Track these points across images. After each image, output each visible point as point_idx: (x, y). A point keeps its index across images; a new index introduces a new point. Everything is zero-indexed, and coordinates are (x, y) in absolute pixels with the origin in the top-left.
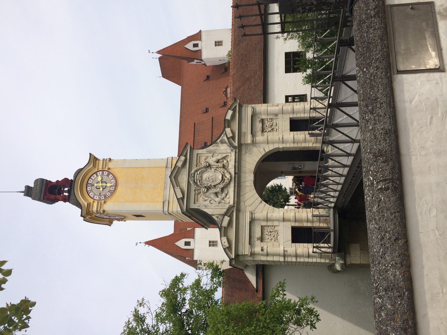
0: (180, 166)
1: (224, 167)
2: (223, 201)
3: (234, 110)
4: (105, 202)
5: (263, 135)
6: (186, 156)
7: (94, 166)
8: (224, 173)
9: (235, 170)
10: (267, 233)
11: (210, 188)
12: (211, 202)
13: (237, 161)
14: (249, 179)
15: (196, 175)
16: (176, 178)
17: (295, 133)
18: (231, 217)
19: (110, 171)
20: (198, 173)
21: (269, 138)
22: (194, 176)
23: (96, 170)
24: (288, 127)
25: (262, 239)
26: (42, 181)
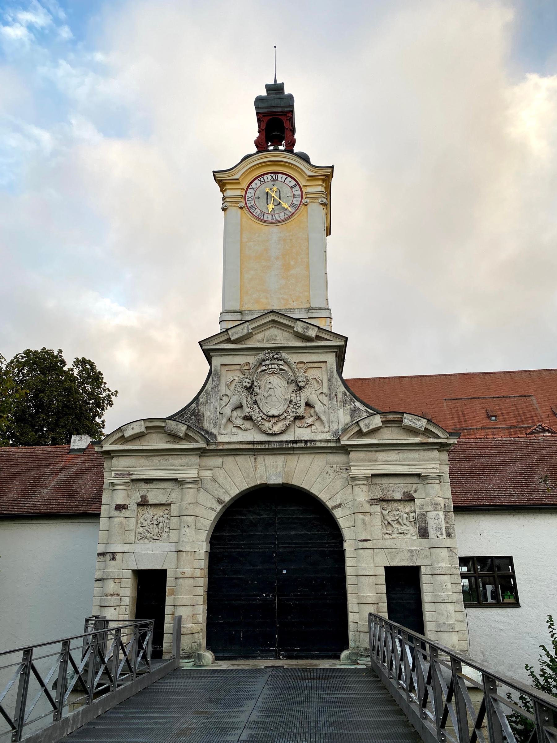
0: (295, 329)
2: (224, 421)
4: (241, 208)
6: (318, 338)
7: (311, 178)
8: (285, 418)
9: (288, 442)
12: (224, 398)
14: (272, 471)
15: (276, 362)
17: (383, 580)
20: (282, 367)
22: (275, 359)
23: (302, 183)
24: (396, 563)
25: (144, 503)
26: (291, 106)
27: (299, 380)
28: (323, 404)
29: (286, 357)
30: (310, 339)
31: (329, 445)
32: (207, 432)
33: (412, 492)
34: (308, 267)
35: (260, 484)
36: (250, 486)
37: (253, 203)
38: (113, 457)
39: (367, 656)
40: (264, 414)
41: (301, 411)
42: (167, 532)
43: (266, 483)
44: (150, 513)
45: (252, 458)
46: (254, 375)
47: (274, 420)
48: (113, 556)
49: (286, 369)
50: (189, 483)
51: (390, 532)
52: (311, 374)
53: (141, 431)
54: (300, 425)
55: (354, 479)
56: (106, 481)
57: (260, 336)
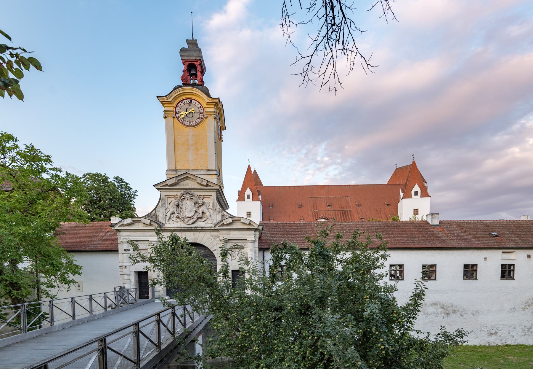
2: (167, 218)
6: (207, 185)
32: (160, 223)
48: (126, 267)
56: (119, 242)
57: (182, 183)
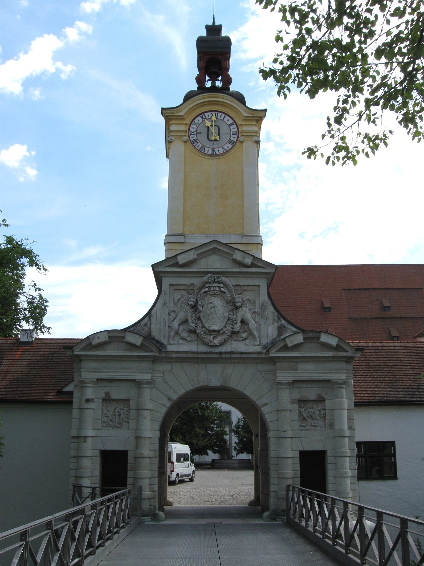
1: (234, 333)
2: (172, 333)
3: (338, 348)
4: (185, 142)
5: (293, 401)
6: (253, 265)
7: (246, 119)
8: (224, 333)
9: (226, 353)
10: (117, 410)
11: (196, 311)
12: (172, 314)
13: (244, 356)
14: (212, 376)
15: (217, 285)
16: (214, 251)
17: (298, 461)
18: (141, 347)
19: (238, 144)
20: (222, 289)
21: (288, 414)
22: (216, 282)
23: (239, 122)
27: (235, 301)
28: (255, 321)
29: (226, 281)
30: (247, 266)
31: (260, 356)
32: (158, 342)
33: (323, 394)
34: (242, 197)
35: (203, 386)
36: (194, 387)
37: (196, 137)
38: (81, 361)
39: (283, 516)
40: (206, 328)
41: (238, 326)
42: (127, 422)
43: (208, 386)
44: (112, 407)
45: (196, 365)
46: (198, 295)
47: (214, 334)
49: (226, 291)
50: (144, 384)
51: (305, 425)
52: (247, 295)
53: (105, 340)
54: (236, 339)
55: (279, 383)
57: (203, 262)
